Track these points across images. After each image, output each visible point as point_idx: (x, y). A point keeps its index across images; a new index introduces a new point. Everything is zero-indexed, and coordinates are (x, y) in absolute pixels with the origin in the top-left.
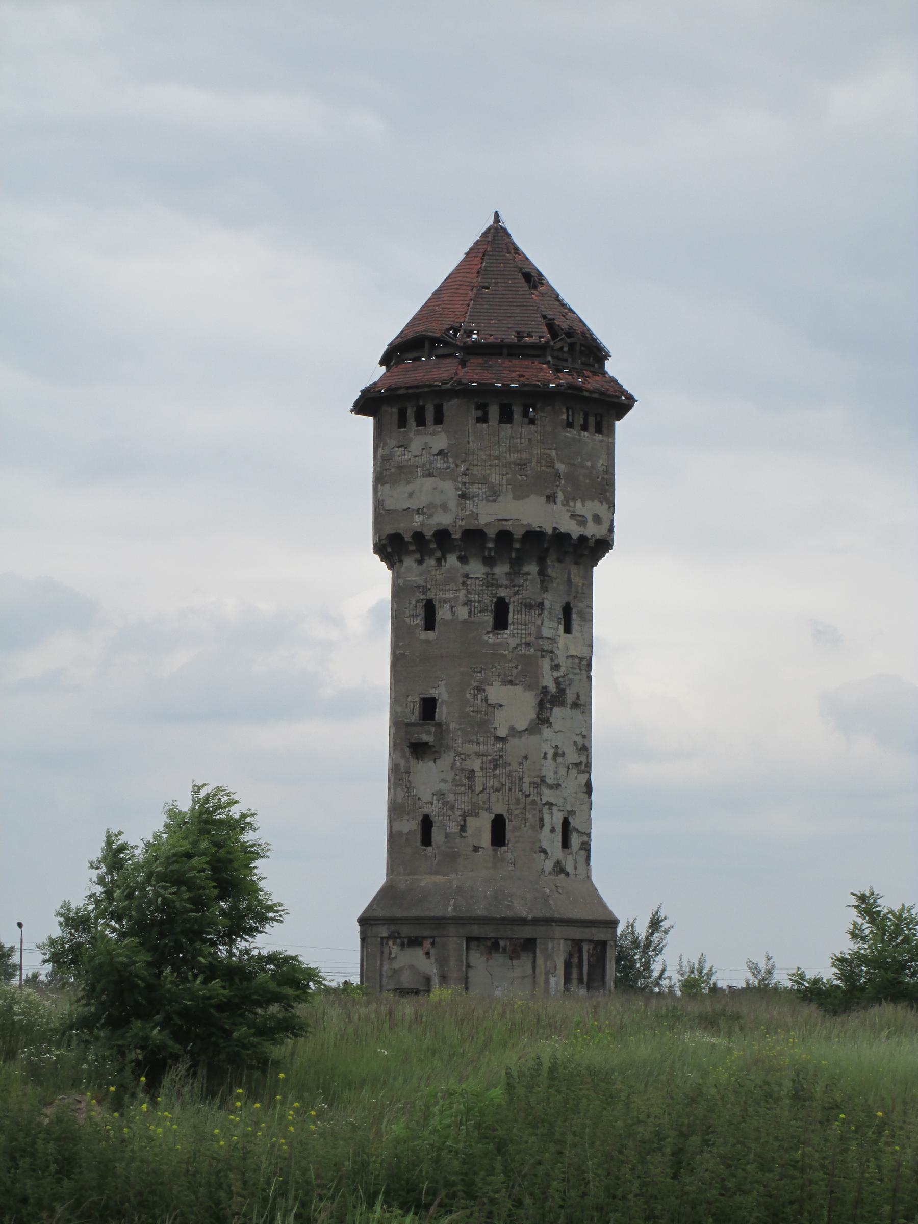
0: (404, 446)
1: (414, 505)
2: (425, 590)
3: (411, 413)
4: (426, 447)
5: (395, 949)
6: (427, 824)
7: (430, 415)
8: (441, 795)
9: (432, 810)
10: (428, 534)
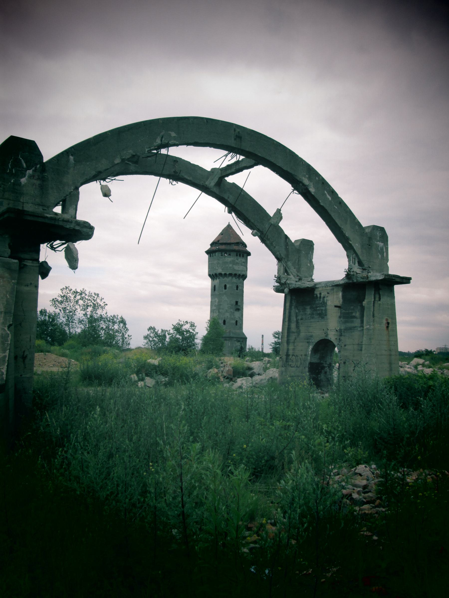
0: (237, 260)
1: (239, 269)
2: (237, 283)
3: (238, 254)
4: (241, 260)
5: (236, 343)
6: (236, 322)
7: (241, 255)
8: (239, 317)
9: (238, 320)
10: (241, 275)
